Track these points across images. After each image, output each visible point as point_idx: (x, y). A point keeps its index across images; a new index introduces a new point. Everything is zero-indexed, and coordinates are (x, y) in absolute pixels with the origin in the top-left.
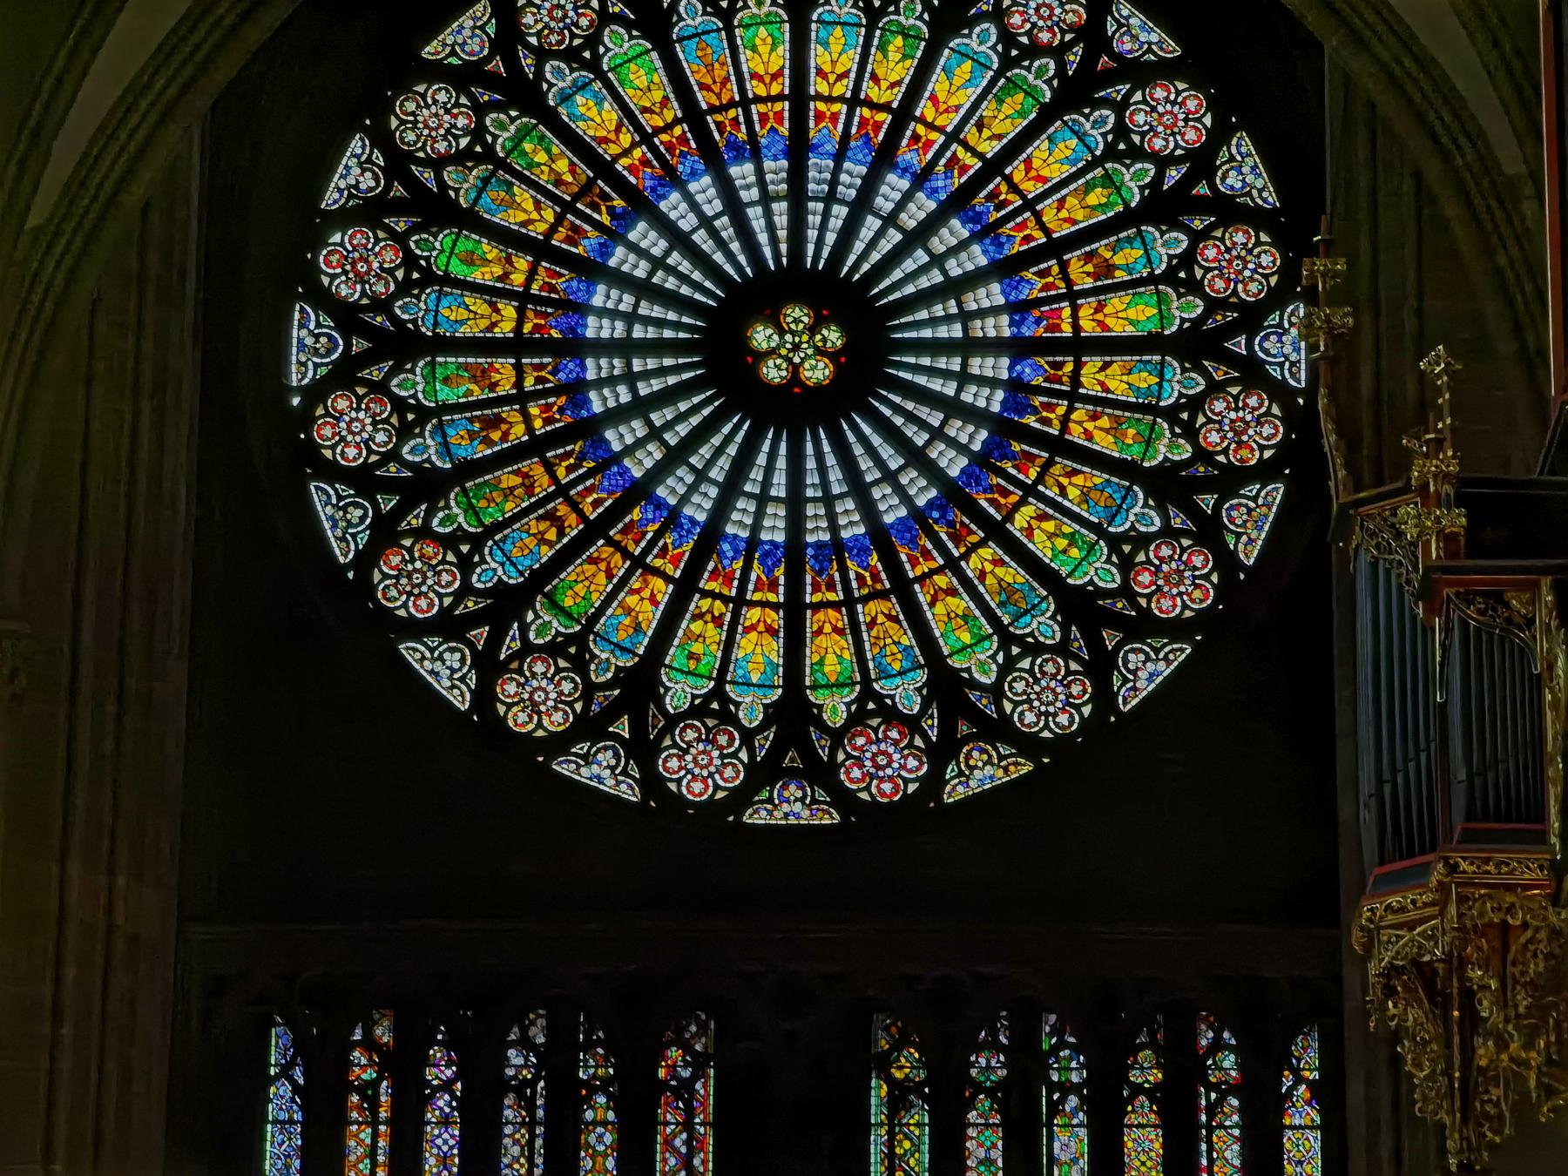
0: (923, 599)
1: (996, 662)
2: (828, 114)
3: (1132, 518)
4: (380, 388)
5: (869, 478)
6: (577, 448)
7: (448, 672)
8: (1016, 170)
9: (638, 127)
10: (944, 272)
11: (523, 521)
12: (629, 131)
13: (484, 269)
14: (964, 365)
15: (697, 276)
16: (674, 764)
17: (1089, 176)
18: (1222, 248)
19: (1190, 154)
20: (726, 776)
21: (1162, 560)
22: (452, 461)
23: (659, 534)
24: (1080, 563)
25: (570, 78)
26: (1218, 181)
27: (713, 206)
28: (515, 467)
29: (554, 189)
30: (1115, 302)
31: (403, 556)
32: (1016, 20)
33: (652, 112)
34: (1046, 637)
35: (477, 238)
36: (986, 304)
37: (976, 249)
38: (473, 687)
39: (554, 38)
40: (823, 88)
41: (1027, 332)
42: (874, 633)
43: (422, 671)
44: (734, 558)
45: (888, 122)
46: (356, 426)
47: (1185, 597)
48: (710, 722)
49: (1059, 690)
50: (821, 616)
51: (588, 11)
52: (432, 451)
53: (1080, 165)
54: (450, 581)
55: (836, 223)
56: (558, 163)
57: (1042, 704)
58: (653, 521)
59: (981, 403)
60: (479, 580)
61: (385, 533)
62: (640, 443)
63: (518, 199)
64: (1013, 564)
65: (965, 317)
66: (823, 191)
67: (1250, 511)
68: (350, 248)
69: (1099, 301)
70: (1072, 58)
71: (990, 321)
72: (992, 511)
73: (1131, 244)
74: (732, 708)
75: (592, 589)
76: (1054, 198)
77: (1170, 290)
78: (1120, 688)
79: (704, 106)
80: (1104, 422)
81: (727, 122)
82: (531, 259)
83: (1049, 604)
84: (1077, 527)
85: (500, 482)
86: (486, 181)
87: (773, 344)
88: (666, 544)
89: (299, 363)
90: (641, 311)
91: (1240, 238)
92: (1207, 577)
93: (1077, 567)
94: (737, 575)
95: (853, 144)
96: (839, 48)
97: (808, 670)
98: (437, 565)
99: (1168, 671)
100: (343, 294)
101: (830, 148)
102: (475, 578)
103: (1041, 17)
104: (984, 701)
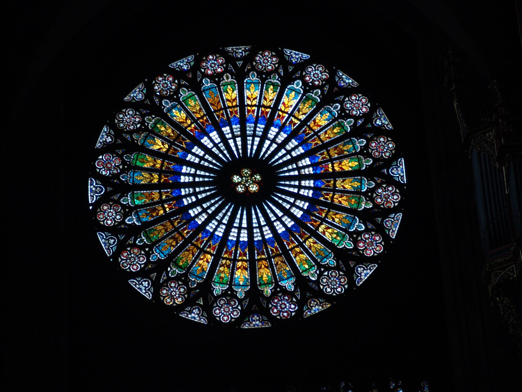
0: (292, 256)
1: (317, 273)
2: (251, 110)
3: (356, 226)
4: (118, 202)
5: (273, 220)
6: (180, 216)
7: (144, 288)
8: (311, 123)
9: (192, 118)
10: (291, 155)
11: (165, 240)
12: (190, 119)
13: (147, 164)
14: (300, 183)
15: (214, 161)
16: (218, 311)
17: (334, 124)
18: (377, 143)
19: (364, 114)
20: (234, 314)
21: (366, 239)
22: (141, 223)
23: (208, 241)
24: (341, 241)
25: (170, 104)
26: (374, 123)
27: (217, 140)
28: (161, 223)
29: (168, 138)
30: (345, 162)
31: (128, 253)
32: (307, 78)
33: (196, 113)
34: (332, 265)
35: (145, 154)
36: (305, 164)
37: (300, 148)
38: (152, 292)
39: (164, 93)
40: (249, 102)
41: (318, 172)
42: (278, 267)
43: (136, 288)
44: (232, 247)
45: (270, 111)
46: (110, 214)
47: (374, 250)
48: (228, 298)
49: (337, 281)
50: (260, 263)
51: (175, 84)
52: (135, 220)
53: (331, 121)
54: (143, 260)
55: (256, 143)
56: (168, 130)
57: (332, 285)
58: (206, 237)
59: (306, 194)
60: (152, 259)
61: (121, 247)
62: (200, 214)
63: (157, 142)
64: (319, 243)
65: (299, 169)
66: (251, 133)
67: (392, 222)
68: (105, 160)
69: (340, 161)
70: (325, 89)
71: (307, 170)
72: (312, 227)
73: (348, 143)
74: (235, 293)
75: (188, 259)
76: (324, 131)
77: (362, 157)
78: (356, 279)
79: (213, 110)
80: (345, 198)
81: (220, 115)
82: (161, 160)
83: (332, 255)
84: (339, 230)
85: (157, 228)
86: (146, 138)
87: (239, 181)
88: (210, 244)
89: (91, 196)
90: (197, 173)
91: (382, 139)
92: (380, 243)
93: (339, 243)
94: (233, 252)
95: (260, 119)
96: (253, 90)
97: (258, 280)
98: (139, 255)
99: (371, 273)
100: (104, 174)
101: (254, 120)
102: (151, 258)
103: (315, 77)
104: (314, 286)
